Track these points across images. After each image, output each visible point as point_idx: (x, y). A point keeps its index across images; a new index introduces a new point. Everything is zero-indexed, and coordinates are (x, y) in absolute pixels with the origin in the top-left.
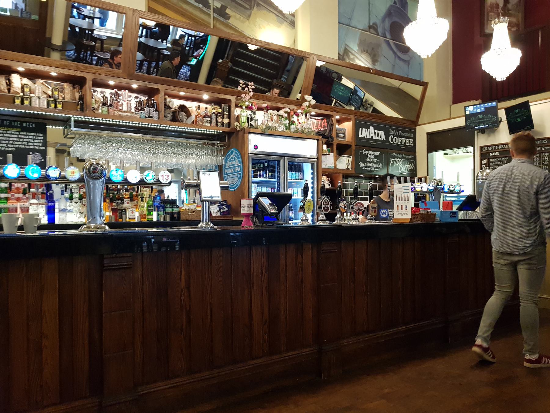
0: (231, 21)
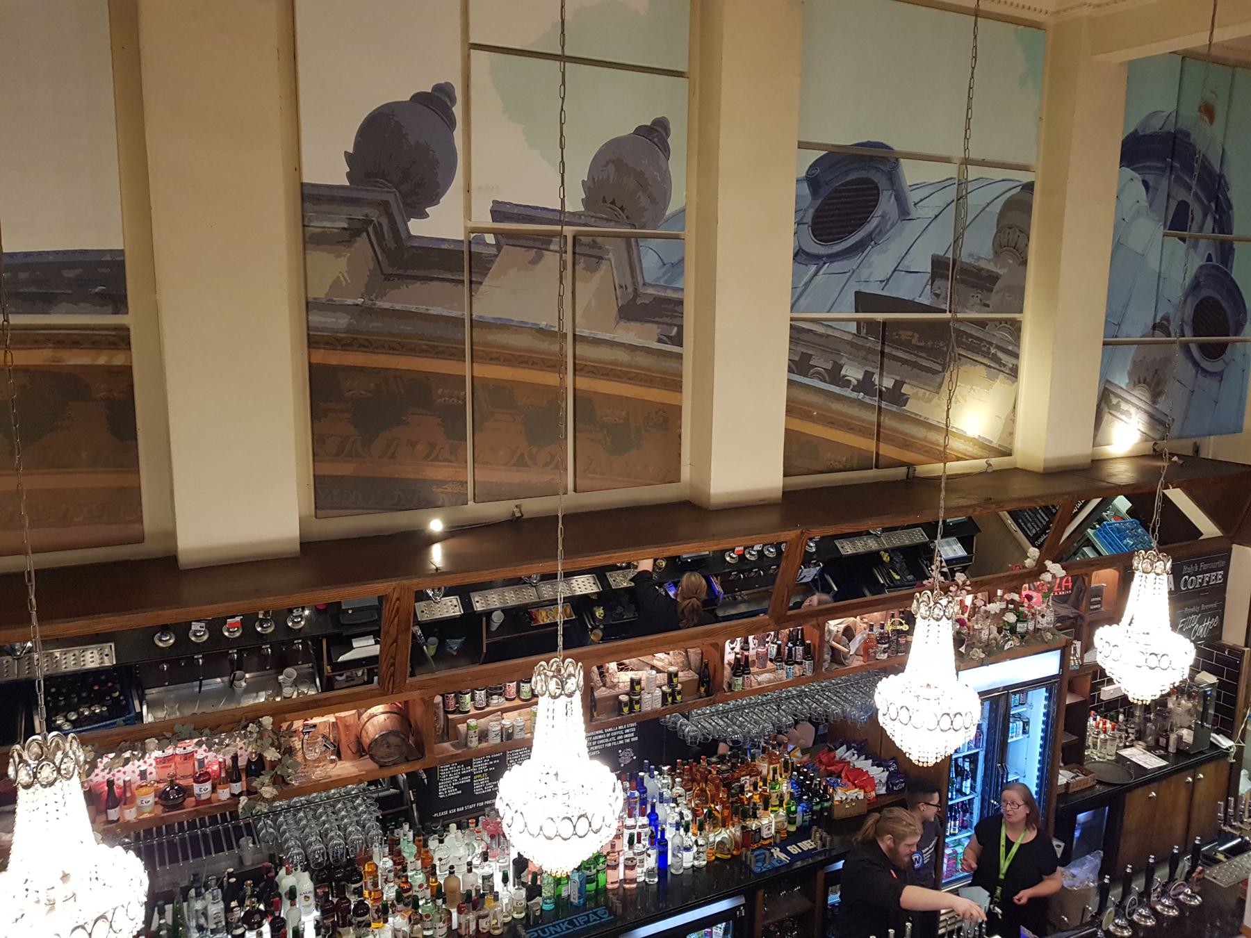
0: (910, 407)
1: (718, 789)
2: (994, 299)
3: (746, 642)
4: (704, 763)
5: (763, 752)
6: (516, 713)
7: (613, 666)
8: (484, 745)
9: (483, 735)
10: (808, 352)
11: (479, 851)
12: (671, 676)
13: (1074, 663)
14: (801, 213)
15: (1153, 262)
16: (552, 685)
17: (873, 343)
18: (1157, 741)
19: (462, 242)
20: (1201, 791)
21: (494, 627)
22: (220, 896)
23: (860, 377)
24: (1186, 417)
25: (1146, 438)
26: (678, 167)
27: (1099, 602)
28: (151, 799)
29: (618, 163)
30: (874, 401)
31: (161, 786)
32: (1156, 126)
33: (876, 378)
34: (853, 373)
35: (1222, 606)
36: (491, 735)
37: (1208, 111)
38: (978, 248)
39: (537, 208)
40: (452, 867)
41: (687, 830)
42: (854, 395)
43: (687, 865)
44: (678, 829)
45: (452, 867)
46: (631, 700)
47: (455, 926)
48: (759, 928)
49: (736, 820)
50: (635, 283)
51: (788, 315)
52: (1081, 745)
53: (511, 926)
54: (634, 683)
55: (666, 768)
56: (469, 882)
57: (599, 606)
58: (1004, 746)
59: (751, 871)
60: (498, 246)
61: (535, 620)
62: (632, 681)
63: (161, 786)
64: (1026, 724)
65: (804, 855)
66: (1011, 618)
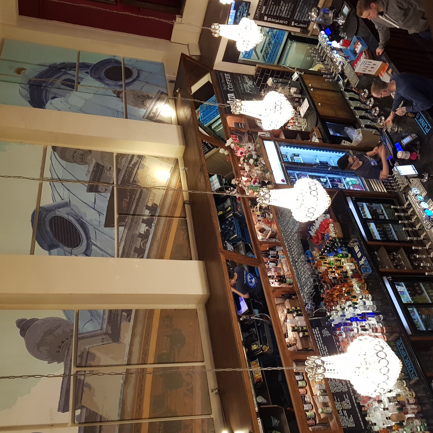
0: (158, 202)
1: (335, 289)
2: (107, 165)
3: (270, 277)
4: (324, 296)
5: (316, 268)
6: (313, 389)
7: (287, 340)
8: (330, 404)
9: (325, 405)
10: (133, 249)
11: (376, 404)
12: (289, 312)
13: (268, 135)
14: (66, 253)
15: (89, 96)
16: (320, 371)
17: (129, 219)
18: (296, 102)
19: (79, 428)
20: (315, 85)
21: (264, 401)
23: (145, 225)
24: (158, 86)
25: (168, 102)
26: (41, 314)
27: (241, 124)
29: (39, 345)
30: (156, 219)
32: (26, 93)
33: (145, 218)
34: (143, 228)
35: (240, 74)
36: (325, 401)
37: (19, 71)
38: (83, 172)
39: (62, 388)
40: (387, 418)
41: (356, 304)
42: (153, 228)
43: (371, 303)
44: (357, 308)
45: (387, 418)
46: (302, 331)
47: (413, 416)
48: (396, 270)
49: (349, 281)
50: (101, 335)
51: (116, 259)
52: (300, 132)
53: (410, 387)
54: (294, 330)
55: (328, 314)
56: (393, 411)
57: (251, 347)
58: (304, 164)
59: (372, 274)
60: (82, 407)
61: (260, 380)
62: (293, 331)
64: (295, 155)
65: (361, 250)
66: (251, 161)
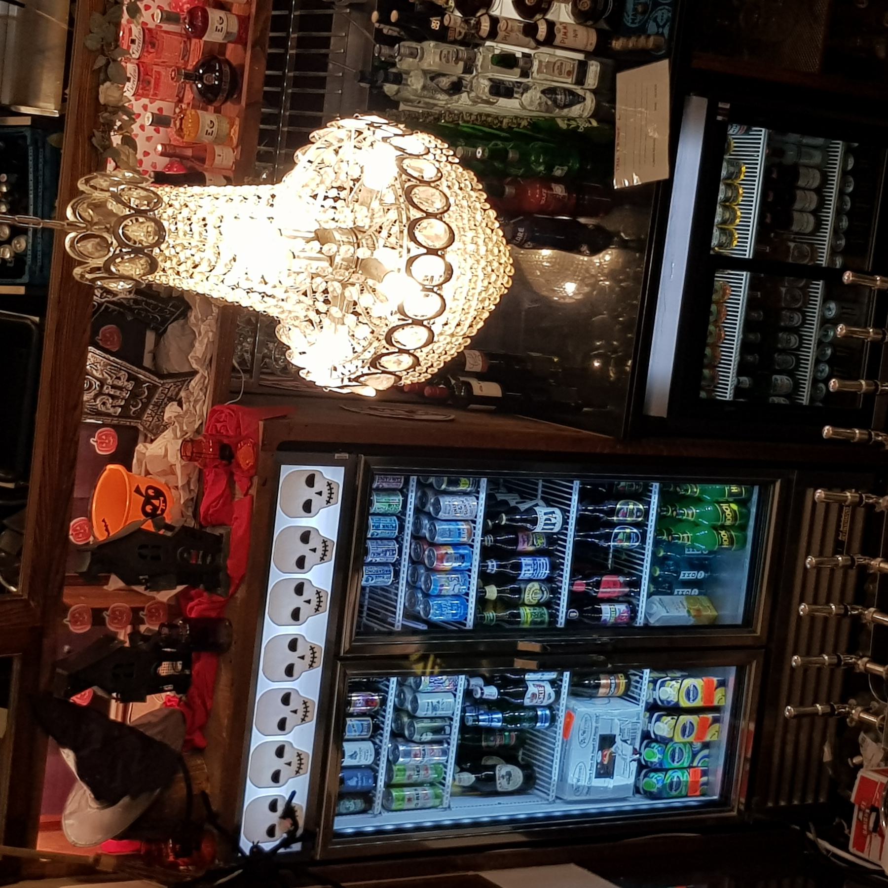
22: (414, 44)
28: (207, 117)
31: (189, 96)
63: (189, 96)
